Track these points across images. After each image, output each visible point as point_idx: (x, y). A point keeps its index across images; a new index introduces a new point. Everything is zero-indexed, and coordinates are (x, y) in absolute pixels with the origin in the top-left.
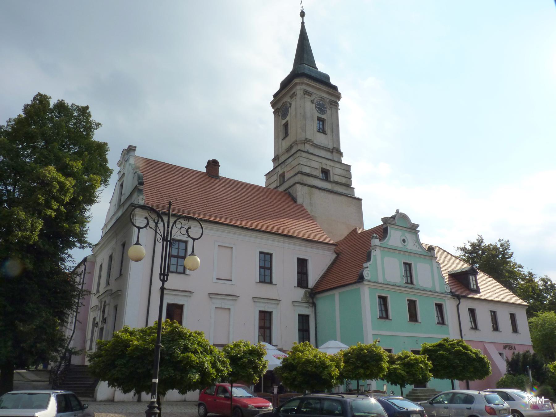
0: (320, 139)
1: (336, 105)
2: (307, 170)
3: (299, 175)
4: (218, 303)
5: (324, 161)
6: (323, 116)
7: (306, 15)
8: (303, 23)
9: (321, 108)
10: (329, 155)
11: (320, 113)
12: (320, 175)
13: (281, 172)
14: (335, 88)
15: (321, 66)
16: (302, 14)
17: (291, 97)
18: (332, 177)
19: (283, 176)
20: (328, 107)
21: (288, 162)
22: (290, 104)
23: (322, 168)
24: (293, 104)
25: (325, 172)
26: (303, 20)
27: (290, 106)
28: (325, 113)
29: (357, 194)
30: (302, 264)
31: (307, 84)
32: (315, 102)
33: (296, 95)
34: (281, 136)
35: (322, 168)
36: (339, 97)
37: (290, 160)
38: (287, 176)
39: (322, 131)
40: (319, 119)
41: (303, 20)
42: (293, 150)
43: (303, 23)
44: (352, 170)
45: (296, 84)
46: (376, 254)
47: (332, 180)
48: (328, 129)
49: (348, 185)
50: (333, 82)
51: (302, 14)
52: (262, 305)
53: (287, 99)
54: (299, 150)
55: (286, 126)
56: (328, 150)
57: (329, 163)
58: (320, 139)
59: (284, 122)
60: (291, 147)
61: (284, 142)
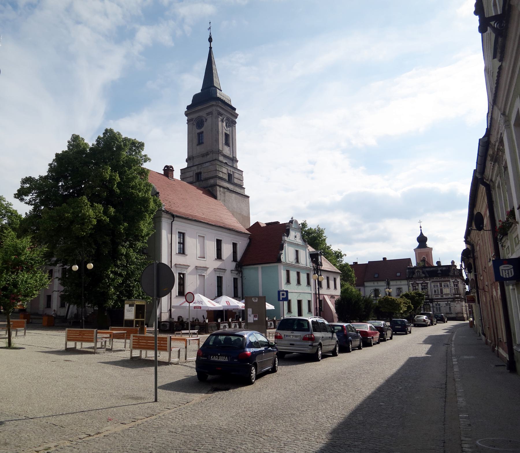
1: (235, 123)
2: (221, 175)
4: (200, 272)
8: (211, 48)
13: (199, 171)
14: (235, 109)
16: (210, 40)
17: (208, 114)
21: (205, 165)
22: (206, 119)
23: (228, 173)
24: (209, 120)
29: (247, 193)
30: (235, 245)
34: (196, 141)
35: (228, 173)
36: (236, 116)
37: (207, 164)
38: (204, 176)
39: (227, 144)
42: (209, 158)
43: (211, 48)
44: (244, 175)
45: (212, 105)
46: (286, 245)
49: (241, 187)
51: (210, 40)
52: (218, 273)
53: (203, 114)
55: (200, 135)
57: (232, 170)
60: (207, 154)
61: (198, 147)
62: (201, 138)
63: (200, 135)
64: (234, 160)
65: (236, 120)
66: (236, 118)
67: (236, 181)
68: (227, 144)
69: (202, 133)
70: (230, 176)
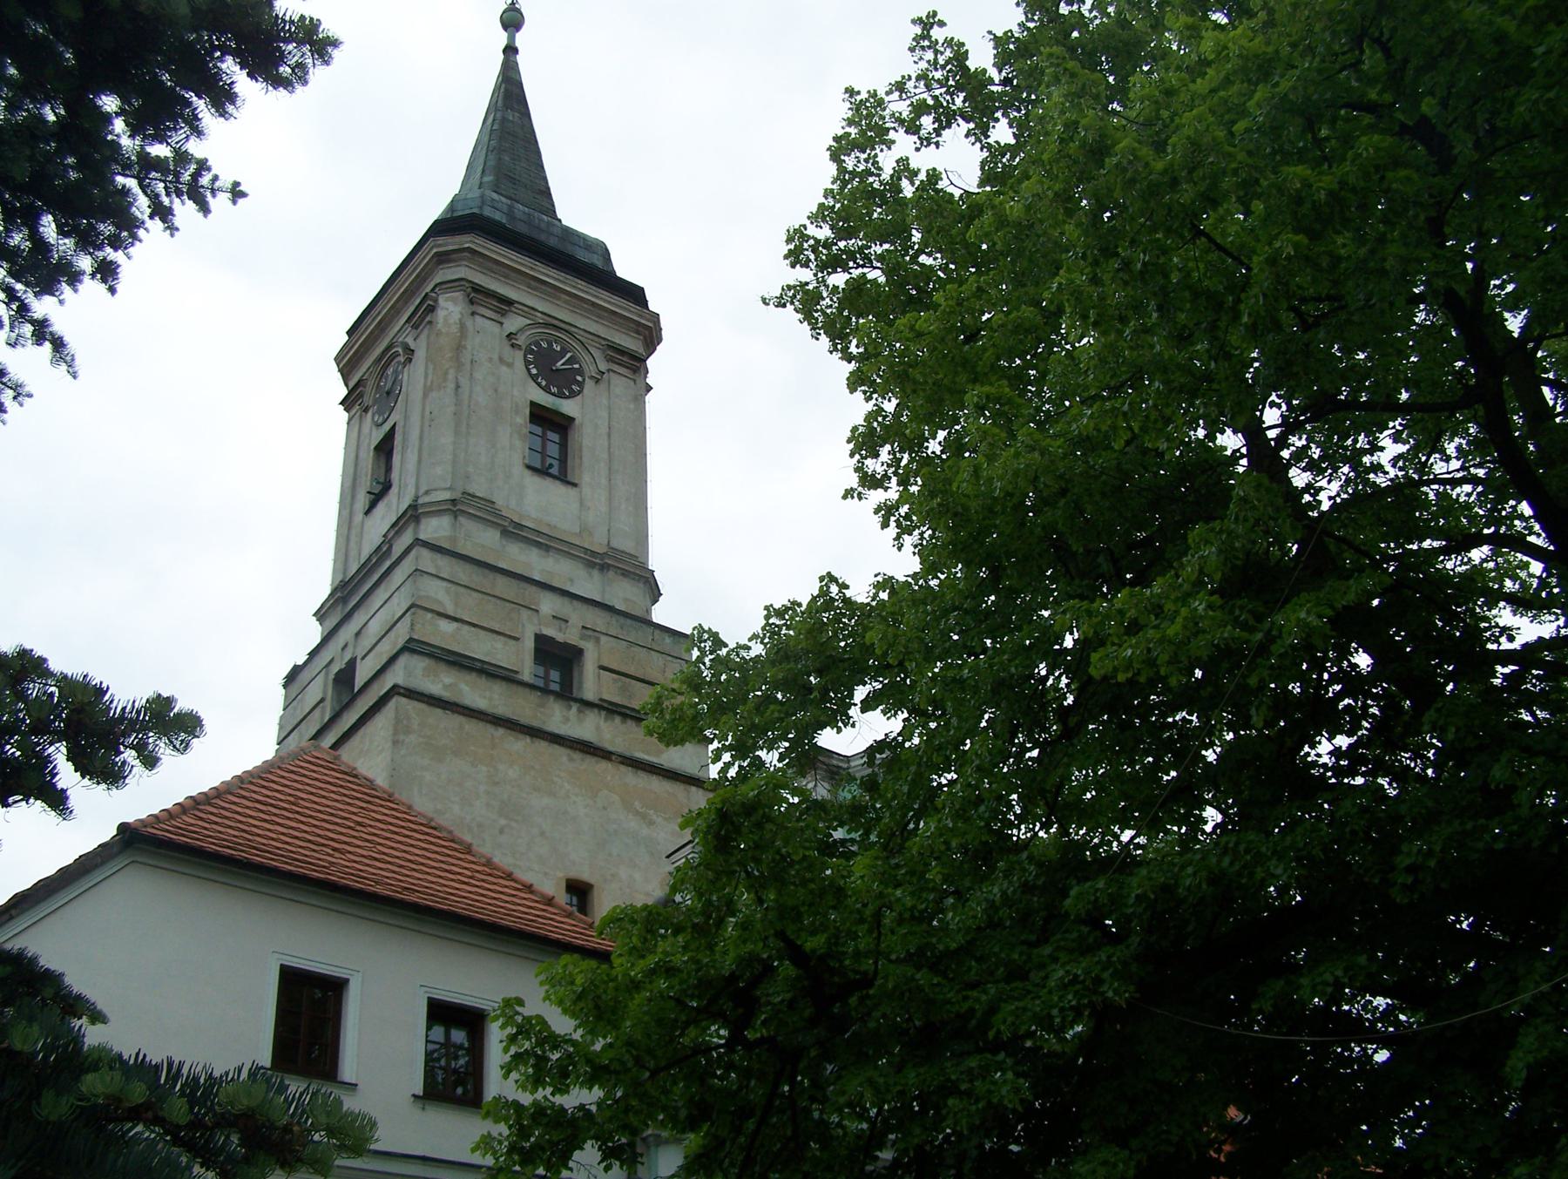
5: (549, 604)
6: (568, 407)
8: (510, 50)
9: (552, 366)
10: (588, 585)
11: (546, 389)
12: (528, 670)
14: (635, 294)
15: (578, 207)
16: (512, 21)
18: (591, 684)
19: (344, 678)
20: (590, 370)
25: (558, 658)
26: (512, 38)
28: (573, 395)
32: (522, 340)
36: (651, 334)
40: (541, 417)
41: (512, 38)
43: (510, 50)
47: (589, 693)
50: (624, 268)
51: (512, 21)
55: (385, 449)
57: (579, 616)
58: (540, 501)
63: (385, 449)
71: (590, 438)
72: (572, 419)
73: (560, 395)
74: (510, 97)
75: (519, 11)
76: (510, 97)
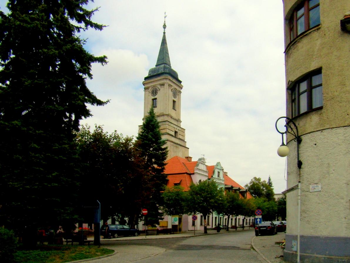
0: (173, 113)
1: (180, 92)
3: (167, 135)
6: (175, 100)
7: (167, 27)
8: (164, 33)
10: (175, 123)
12: (173, 133)
14: (180, 82)
15: (174, 67)
16: (165, 27)
23: (175, 131)
26: (164, 30)
27: (159, 90)
31: (170, 80)
33: (164, 85)
35: (175, 131)
41: (164, 30)
43: (164, 33)
47: (178, 138)
48: (176, 108)
50: (180, 79)
51: (165, 27)
54: (167, 121)
56: (175, 120)
59: (153, 98)
62: (154, 103)
64: (179, 121)
65: (182, 90)
66: (182, 88)
67: (181, 137)
68: (174, 108)
69: (156, 99)
70: (176, 132)
71: (177, 104)
72: (176, 101)
73: (175, 98)
74: (164, 42)
75: (166, 26)
76: (164, 42)
